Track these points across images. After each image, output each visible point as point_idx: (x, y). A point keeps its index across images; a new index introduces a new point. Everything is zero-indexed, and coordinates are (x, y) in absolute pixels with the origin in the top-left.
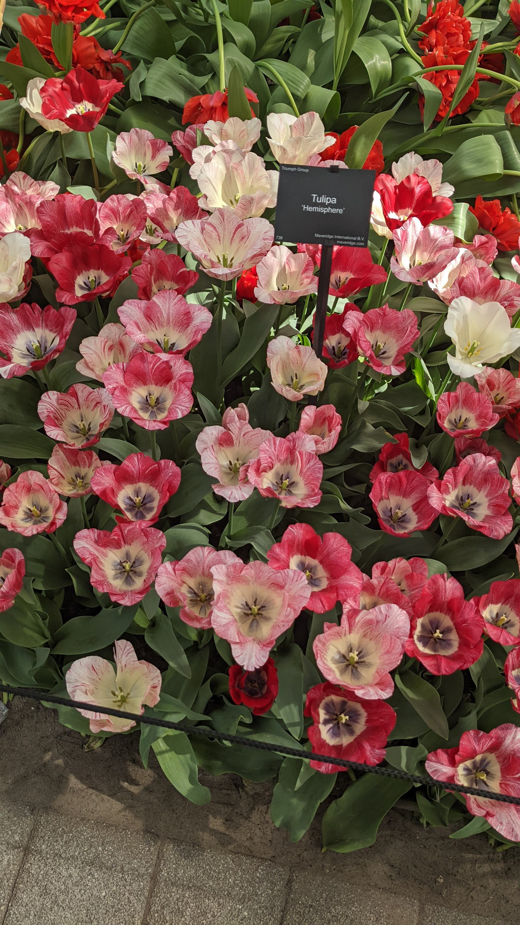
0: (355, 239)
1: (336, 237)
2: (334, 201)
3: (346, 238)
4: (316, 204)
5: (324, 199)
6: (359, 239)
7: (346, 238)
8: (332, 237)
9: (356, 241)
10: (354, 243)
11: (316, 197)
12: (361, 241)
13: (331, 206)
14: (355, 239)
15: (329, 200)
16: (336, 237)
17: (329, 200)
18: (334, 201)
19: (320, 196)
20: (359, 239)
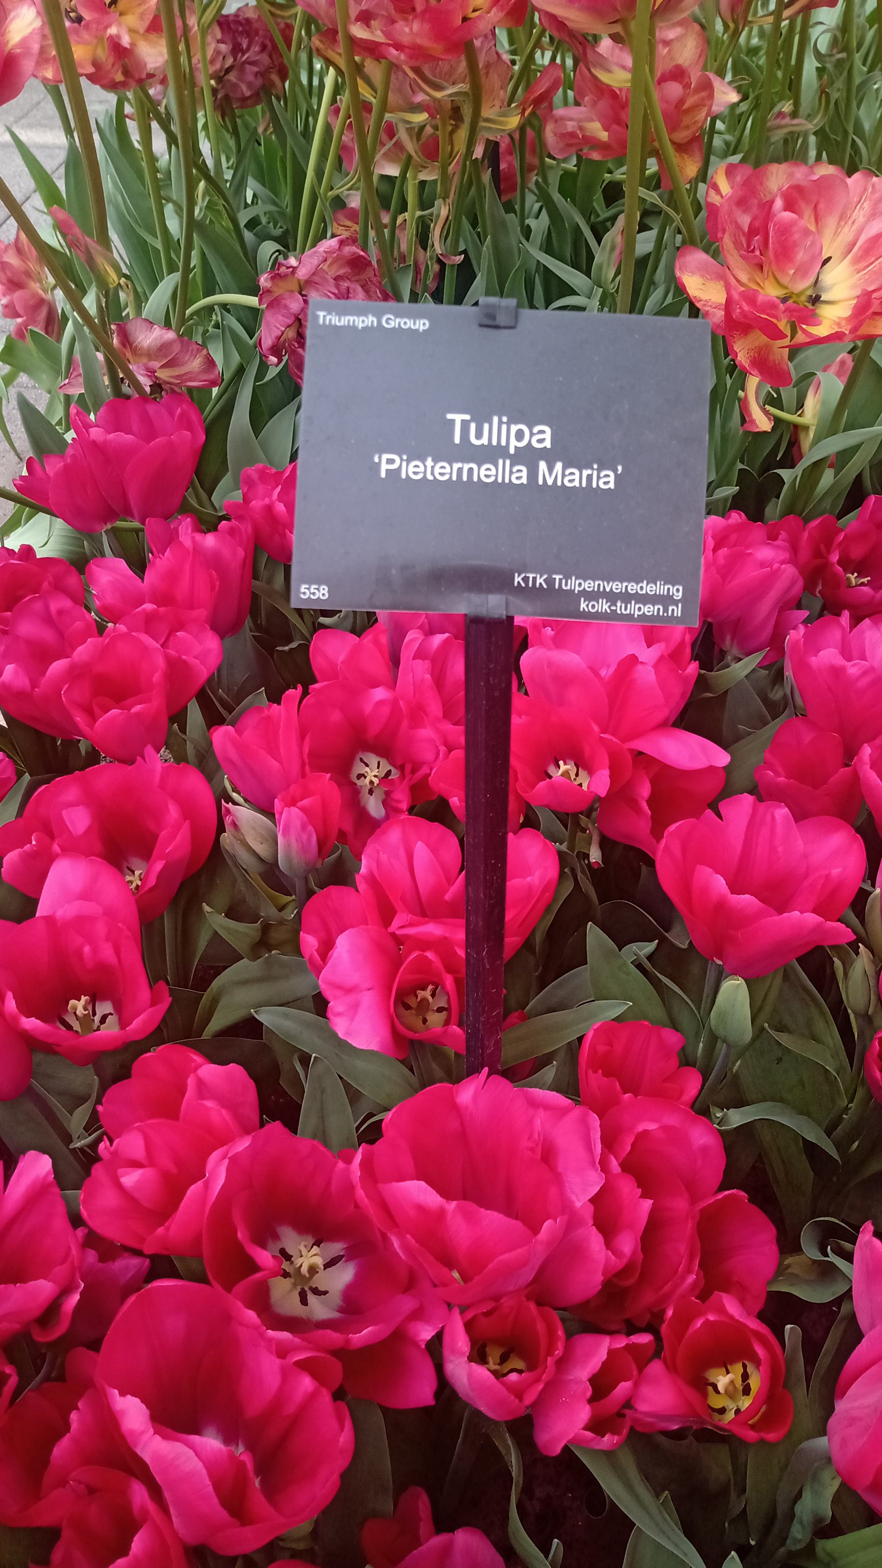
5: (500, 431)
11: (465, 425)
13: (528, 457)
15: (520, 435)
17: (520, 435)
18: (543, 436)
19: (481, 418)
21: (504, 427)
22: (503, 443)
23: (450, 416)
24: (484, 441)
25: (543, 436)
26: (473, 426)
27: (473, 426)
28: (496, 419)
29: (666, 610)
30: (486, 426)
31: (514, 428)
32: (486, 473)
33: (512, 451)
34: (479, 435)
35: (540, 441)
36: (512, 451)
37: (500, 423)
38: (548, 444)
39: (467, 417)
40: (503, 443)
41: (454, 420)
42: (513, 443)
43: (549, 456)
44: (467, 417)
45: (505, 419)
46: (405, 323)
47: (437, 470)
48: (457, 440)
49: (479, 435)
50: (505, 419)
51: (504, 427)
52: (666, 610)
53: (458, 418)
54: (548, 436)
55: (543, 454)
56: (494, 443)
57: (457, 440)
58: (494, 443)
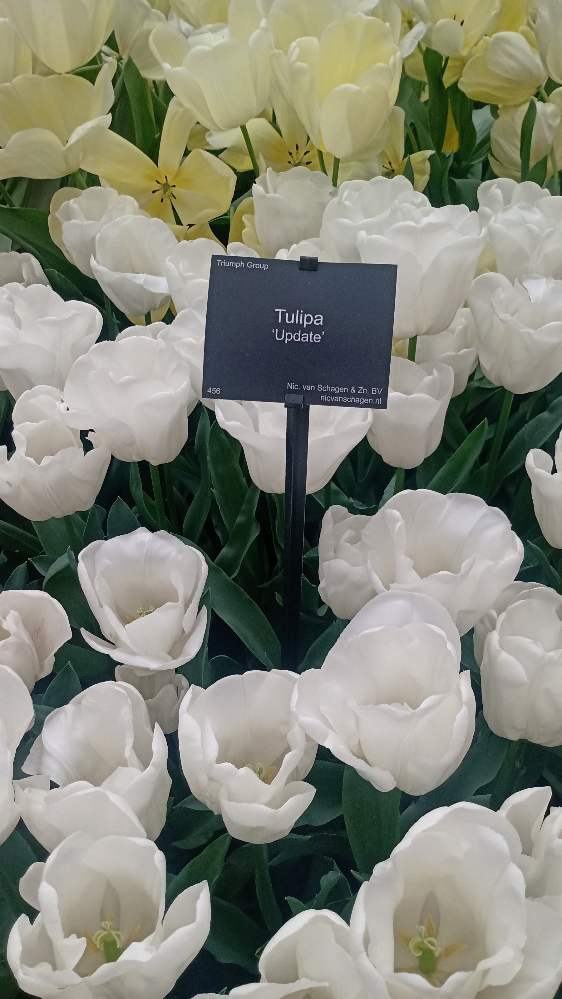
2: (320, 320)
5: (300, 318)
11: (284, 314)
15: (308, 319)
17: (308, 319)
19: (291, 311)
21: (301, 315)
22: (301, 323)
23: (276, 310)
25: (320, 320)
26: (287, 314)
27: (287, 314)
28: (298, 311)
29: (374, 401)
30: (293, 315)
33: (305, 327)
34: (290, 319)
35: (317, 322)
36: (305, 327)
37: (300, 313)
38: (321, 323)
39: (285, 310)
40: (301, 323)
41: (279, 312)
42: (305, 322)
44: (285, 310)
45: (302, 312)
46: (257, 266)
47: (315, 338)
48: (280, 322)
49: (290, 319)
50: (302, 312)
51: (301, 315)
52: (374, 401)
53: (280, 311)
54: (321, 319)
56: (297, 323)
57: (280, 322)
58: (297, 323)
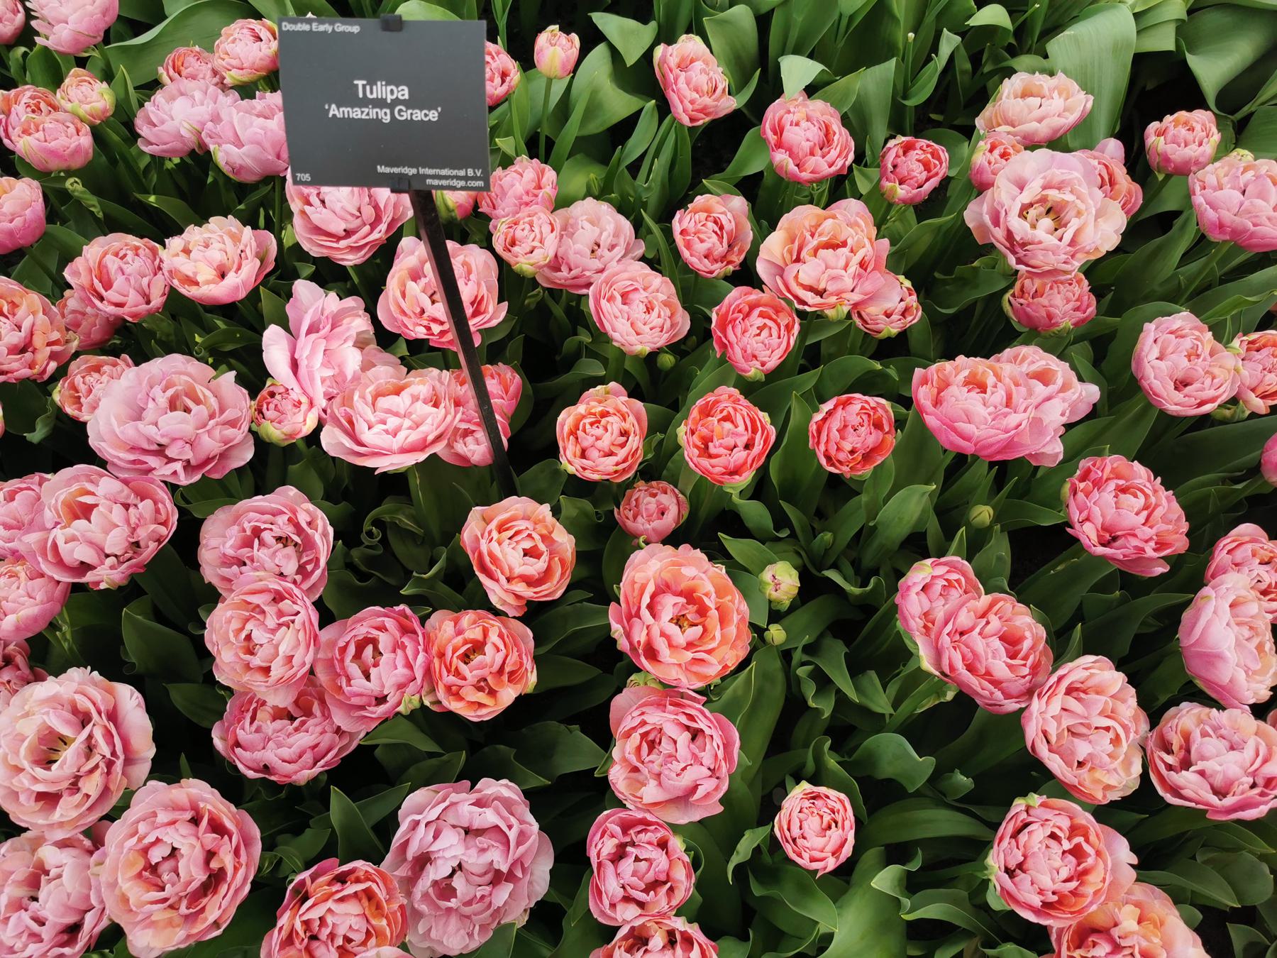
0: (462, 173)
1: (422, 171)
3: (444, 172)
4: (365, 102)
5: (382, 90)
6: (470, 172)
7: (444, 172)
8: (412, 171)
9: (466, 178)
10: (462, 183)
11: (364, 86)
12: (475, 178)
14: (462, 173)
15: (392, 92)
16: (422, 171)
17: (392, 92)
18: (404, 92)
19: (372, 83)
20: (470, 172)
24: (374, 96)
25: (404, 92)
26: (368, 88)
27: (368, 88)
31: (389, 88)
32: (372, 113)
34: (372, 93)
38: (407, 97)
43: (409, 104)
48: (361, 95)
49: (372, 93)
53: (360, 83)
54: (406, 92)
55: (403, 102)
57: (361, 95)
